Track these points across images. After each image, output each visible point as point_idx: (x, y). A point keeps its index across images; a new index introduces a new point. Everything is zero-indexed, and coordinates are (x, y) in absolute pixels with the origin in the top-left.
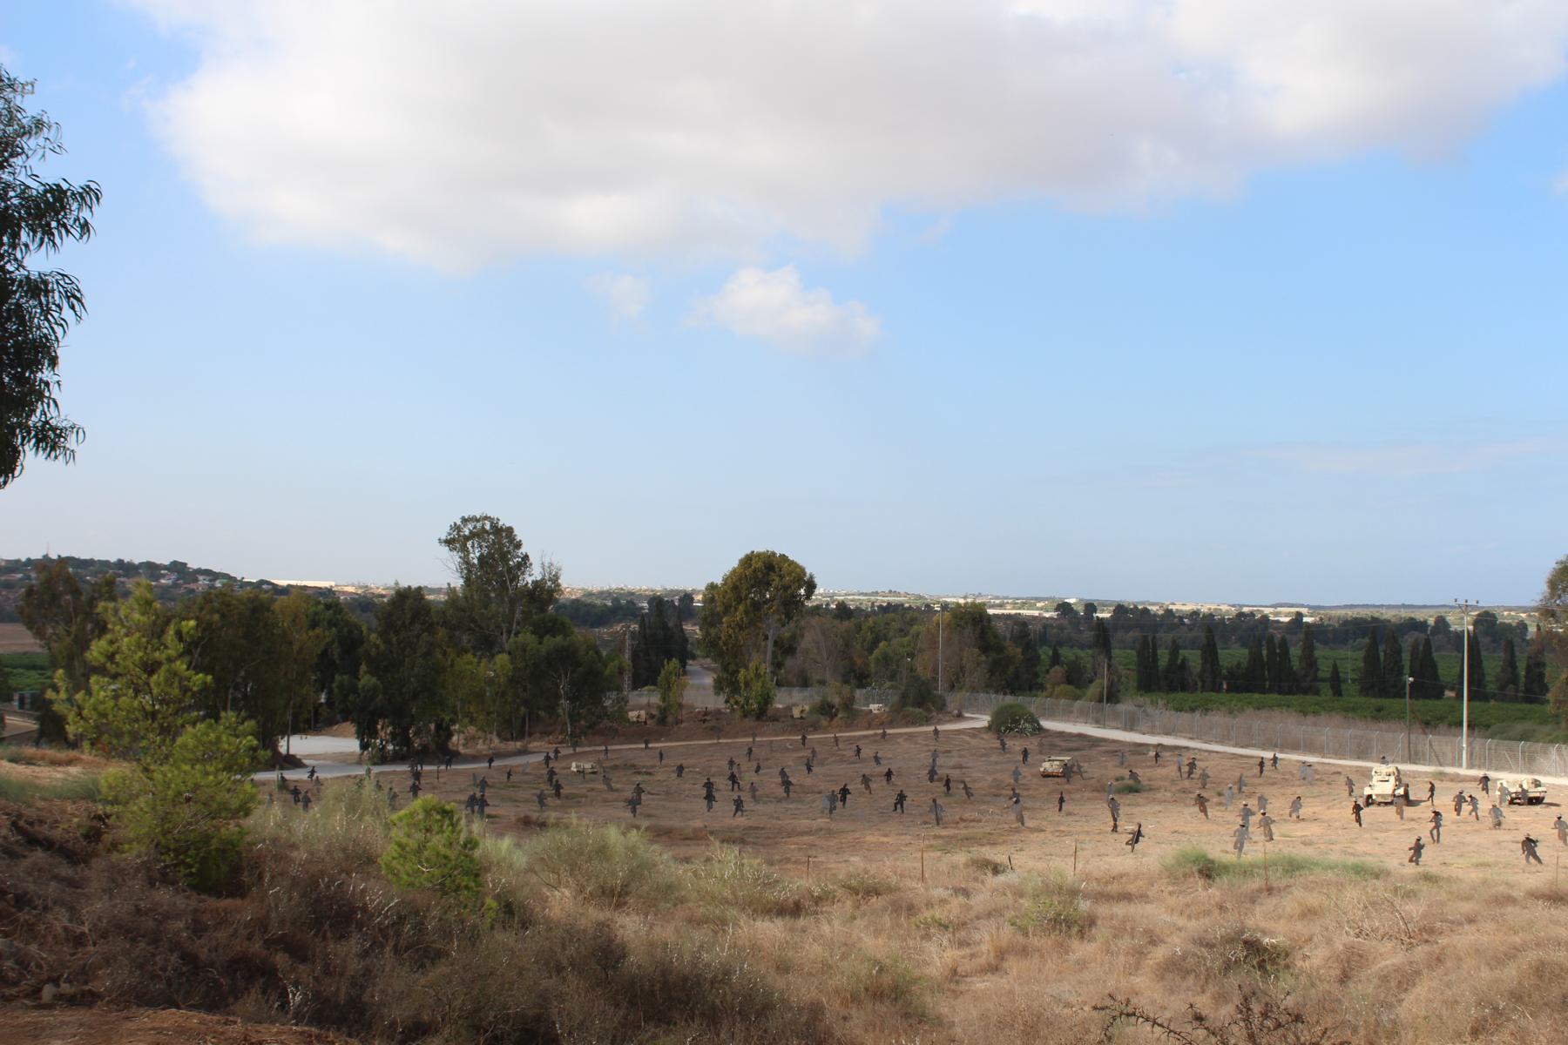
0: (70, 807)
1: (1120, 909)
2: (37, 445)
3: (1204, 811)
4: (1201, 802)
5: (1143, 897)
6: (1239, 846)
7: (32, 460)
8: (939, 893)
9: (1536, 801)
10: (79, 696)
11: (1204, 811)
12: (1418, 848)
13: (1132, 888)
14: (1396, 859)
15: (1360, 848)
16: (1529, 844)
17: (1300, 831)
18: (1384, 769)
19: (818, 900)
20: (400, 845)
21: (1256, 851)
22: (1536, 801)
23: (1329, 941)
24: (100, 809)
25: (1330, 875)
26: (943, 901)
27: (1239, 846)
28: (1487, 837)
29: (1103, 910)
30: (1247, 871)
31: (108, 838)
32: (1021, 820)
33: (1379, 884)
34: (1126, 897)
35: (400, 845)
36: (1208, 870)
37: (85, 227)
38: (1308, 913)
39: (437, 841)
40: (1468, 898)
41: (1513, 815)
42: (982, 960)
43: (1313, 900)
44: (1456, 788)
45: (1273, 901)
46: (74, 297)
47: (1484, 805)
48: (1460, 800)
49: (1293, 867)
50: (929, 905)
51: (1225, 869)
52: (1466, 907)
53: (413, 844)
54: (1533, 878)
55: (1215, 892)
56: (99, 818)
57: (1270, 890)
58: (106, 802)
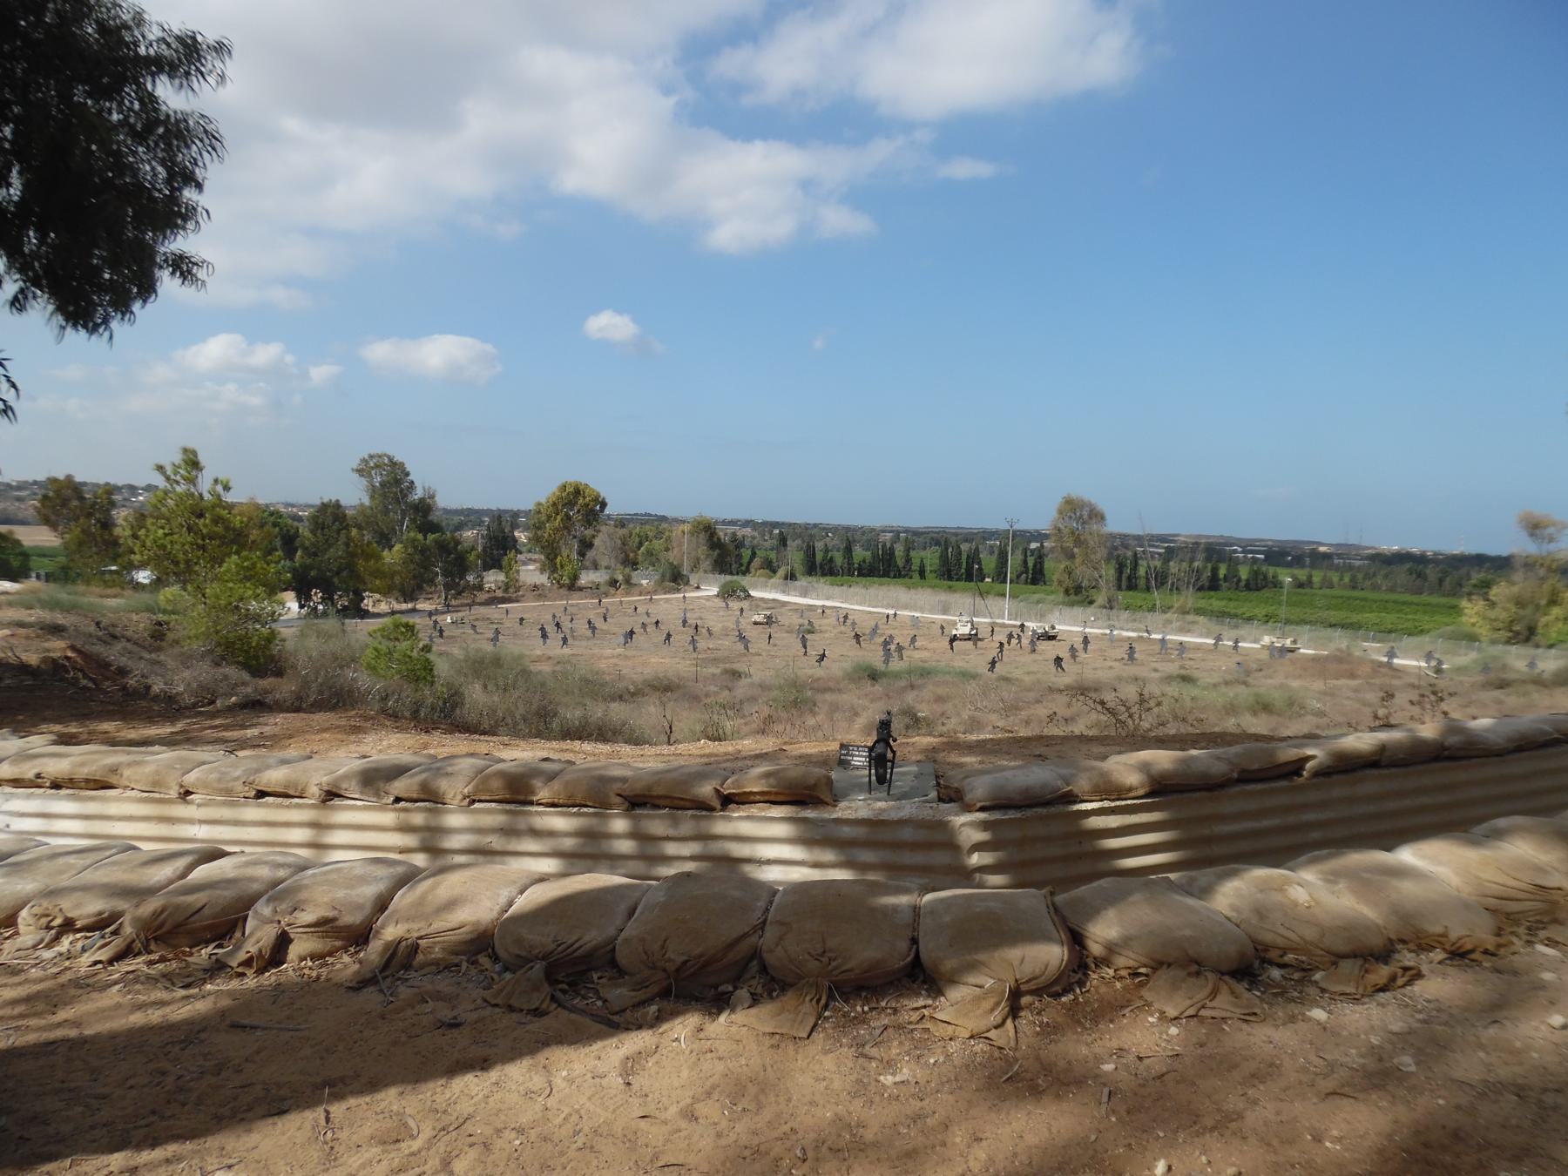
0: (135, 617)
1: (828, 697)
2: (173, 273)
3: (858, 642)
4: (857, 637)
5: (840, 691)
6: (887, 662)
7: (167, 283)
8: (712, 688)
9: (1053, 638)
10: (142, 532)
11: (858, 642)
12: (993, 663)
13: (831, 684)
14: (983, 668)
15: (956, 664)
16: (1058, 660)
17: (917, 655)
18: (965, 619)
19: (633, 695)
20: (376, 649)
21: (896, 665)
22: (1053, 638)
23: (958, 714)
24: (161, 617)
25: (948, 678)
26: (716, 693)
27: (887, 662)
28: (1030, 658)
29: (819, 697)
30: (897, 675)
31: (170, 636)
32: (747, 648)
33: (973, 684)
34: (829, 690)
35: (376, 649)
36: (874, 676)
37: (222, 77)
38: (940, 699)
39: (404, 645)
40: (1030, 690)
41: (1043, 646)
42: (754, 726)
43: (941, 691)
44: (1007, 631)
45: (916, 692)
46: (212, 140)
47: (1025, 642)
48: (1010, 636)
49: (926, 673)
50: (707, 696)
51: (884, 674)
52: (1031, 695)
53: (383, 648)
54: (1065, 680)
55: (878, 688)
56: (160, 624)
57: (912, 687)
58: (165, 612)
